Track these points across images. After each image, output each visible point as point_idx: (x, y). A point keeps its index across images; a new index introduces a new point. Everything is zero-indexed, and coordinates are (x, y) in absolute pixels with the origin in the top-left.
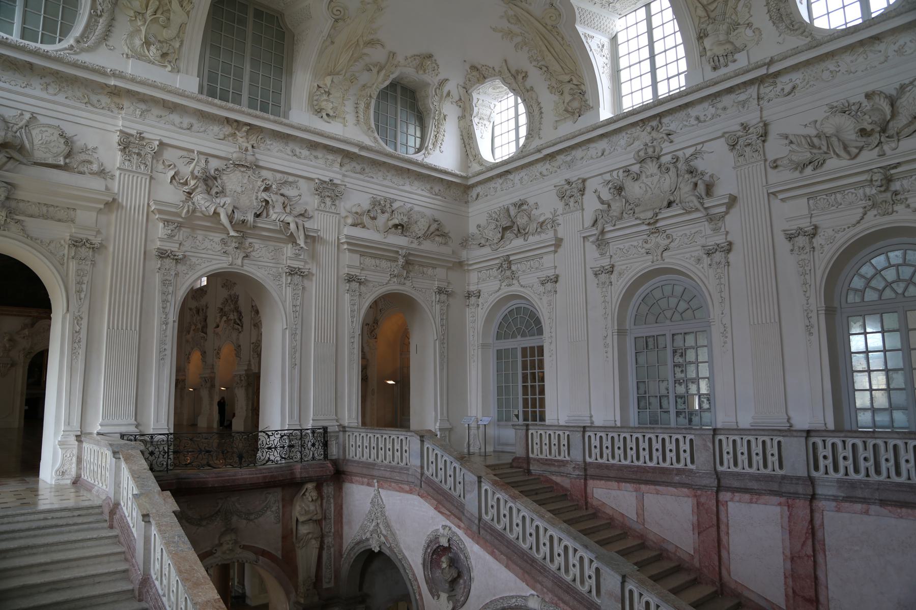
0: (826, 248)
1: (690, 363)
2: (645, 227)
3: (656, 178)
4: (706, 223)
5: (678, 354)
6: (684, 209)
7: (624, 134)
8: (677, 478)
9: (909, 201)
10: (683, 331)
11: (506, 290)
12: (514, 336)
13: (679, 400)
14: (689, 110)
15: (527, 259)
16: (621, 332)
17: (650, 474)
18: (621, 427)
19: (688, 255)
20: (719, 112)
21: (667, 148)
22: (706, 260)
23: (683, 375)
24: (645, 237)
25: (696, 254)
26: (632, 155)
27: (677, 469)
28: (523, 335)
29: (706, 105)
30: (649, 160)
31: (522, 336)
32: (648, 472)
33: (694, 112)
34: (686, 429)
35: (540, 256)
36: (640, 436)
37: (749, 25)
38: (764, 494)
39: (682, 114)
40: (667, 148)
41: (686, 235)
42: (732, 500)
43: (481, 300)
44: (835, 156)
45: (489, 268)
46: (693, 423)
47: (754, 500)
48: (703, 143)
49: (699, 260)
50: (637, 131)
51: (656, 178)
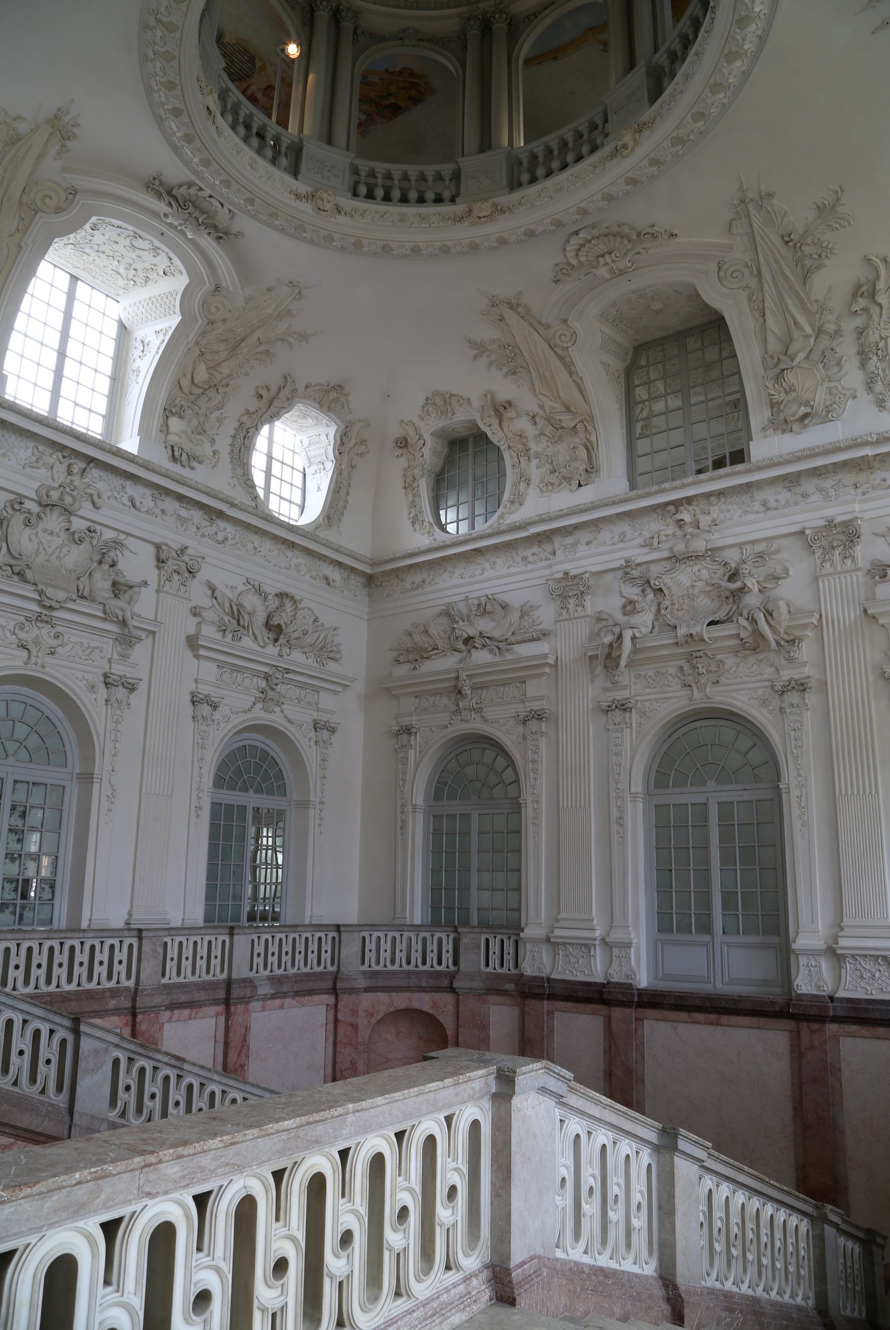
0: (222, 725)
1: (33, 829)
2: (34, 607)
3: (57, 542)
4: (111, 641)
5: (17, 813)
6: (105, 612)
7: (31, 444)
8: (113, 1003)
9: (284, 706)
10: (32, 780)
11: (259, 715)
12: (245, 789)
13: (7, 885)
14: (129, 484)
15: (303, 686)
16: (87, 778)
17: (73, 1004)
18: (66, 931)
19: (79, 675)
20: (157, 511)
21: (86, 509)
22: (102, 690)
23: (19, 847)
24: (22, 619)
25: (90, 677)
26: (36, 485)
27: (110, 990)
28: (259, 791)
29: (148, 492)
30: (57, 510)
31: (256, 792)
32: (71, 1001)
33: (132, 489)
34: (12, 931)
35: (317, 690)
36: (116, 942)
37: (213, 442)
38: (205, 1005)
39: (118, 481)
40: (86, 509)
41: (81, 644)
42: (170, 1020)
43: (217, 715)
44: (252, 637)
45: (255, 673)
46: (25, 921)
47: (193, 1015)
48: (128, 534)
49: (92, 688)
50: (54, 458)
51: (57, 542)
